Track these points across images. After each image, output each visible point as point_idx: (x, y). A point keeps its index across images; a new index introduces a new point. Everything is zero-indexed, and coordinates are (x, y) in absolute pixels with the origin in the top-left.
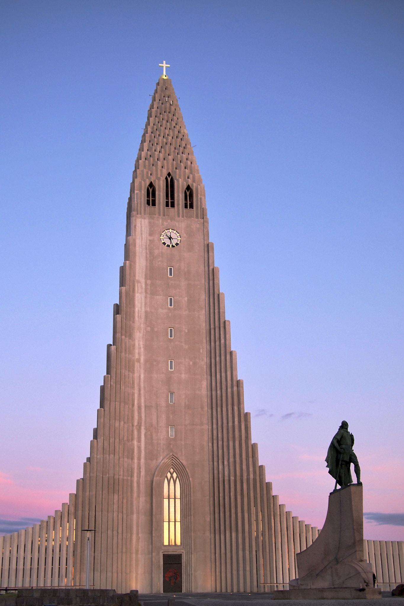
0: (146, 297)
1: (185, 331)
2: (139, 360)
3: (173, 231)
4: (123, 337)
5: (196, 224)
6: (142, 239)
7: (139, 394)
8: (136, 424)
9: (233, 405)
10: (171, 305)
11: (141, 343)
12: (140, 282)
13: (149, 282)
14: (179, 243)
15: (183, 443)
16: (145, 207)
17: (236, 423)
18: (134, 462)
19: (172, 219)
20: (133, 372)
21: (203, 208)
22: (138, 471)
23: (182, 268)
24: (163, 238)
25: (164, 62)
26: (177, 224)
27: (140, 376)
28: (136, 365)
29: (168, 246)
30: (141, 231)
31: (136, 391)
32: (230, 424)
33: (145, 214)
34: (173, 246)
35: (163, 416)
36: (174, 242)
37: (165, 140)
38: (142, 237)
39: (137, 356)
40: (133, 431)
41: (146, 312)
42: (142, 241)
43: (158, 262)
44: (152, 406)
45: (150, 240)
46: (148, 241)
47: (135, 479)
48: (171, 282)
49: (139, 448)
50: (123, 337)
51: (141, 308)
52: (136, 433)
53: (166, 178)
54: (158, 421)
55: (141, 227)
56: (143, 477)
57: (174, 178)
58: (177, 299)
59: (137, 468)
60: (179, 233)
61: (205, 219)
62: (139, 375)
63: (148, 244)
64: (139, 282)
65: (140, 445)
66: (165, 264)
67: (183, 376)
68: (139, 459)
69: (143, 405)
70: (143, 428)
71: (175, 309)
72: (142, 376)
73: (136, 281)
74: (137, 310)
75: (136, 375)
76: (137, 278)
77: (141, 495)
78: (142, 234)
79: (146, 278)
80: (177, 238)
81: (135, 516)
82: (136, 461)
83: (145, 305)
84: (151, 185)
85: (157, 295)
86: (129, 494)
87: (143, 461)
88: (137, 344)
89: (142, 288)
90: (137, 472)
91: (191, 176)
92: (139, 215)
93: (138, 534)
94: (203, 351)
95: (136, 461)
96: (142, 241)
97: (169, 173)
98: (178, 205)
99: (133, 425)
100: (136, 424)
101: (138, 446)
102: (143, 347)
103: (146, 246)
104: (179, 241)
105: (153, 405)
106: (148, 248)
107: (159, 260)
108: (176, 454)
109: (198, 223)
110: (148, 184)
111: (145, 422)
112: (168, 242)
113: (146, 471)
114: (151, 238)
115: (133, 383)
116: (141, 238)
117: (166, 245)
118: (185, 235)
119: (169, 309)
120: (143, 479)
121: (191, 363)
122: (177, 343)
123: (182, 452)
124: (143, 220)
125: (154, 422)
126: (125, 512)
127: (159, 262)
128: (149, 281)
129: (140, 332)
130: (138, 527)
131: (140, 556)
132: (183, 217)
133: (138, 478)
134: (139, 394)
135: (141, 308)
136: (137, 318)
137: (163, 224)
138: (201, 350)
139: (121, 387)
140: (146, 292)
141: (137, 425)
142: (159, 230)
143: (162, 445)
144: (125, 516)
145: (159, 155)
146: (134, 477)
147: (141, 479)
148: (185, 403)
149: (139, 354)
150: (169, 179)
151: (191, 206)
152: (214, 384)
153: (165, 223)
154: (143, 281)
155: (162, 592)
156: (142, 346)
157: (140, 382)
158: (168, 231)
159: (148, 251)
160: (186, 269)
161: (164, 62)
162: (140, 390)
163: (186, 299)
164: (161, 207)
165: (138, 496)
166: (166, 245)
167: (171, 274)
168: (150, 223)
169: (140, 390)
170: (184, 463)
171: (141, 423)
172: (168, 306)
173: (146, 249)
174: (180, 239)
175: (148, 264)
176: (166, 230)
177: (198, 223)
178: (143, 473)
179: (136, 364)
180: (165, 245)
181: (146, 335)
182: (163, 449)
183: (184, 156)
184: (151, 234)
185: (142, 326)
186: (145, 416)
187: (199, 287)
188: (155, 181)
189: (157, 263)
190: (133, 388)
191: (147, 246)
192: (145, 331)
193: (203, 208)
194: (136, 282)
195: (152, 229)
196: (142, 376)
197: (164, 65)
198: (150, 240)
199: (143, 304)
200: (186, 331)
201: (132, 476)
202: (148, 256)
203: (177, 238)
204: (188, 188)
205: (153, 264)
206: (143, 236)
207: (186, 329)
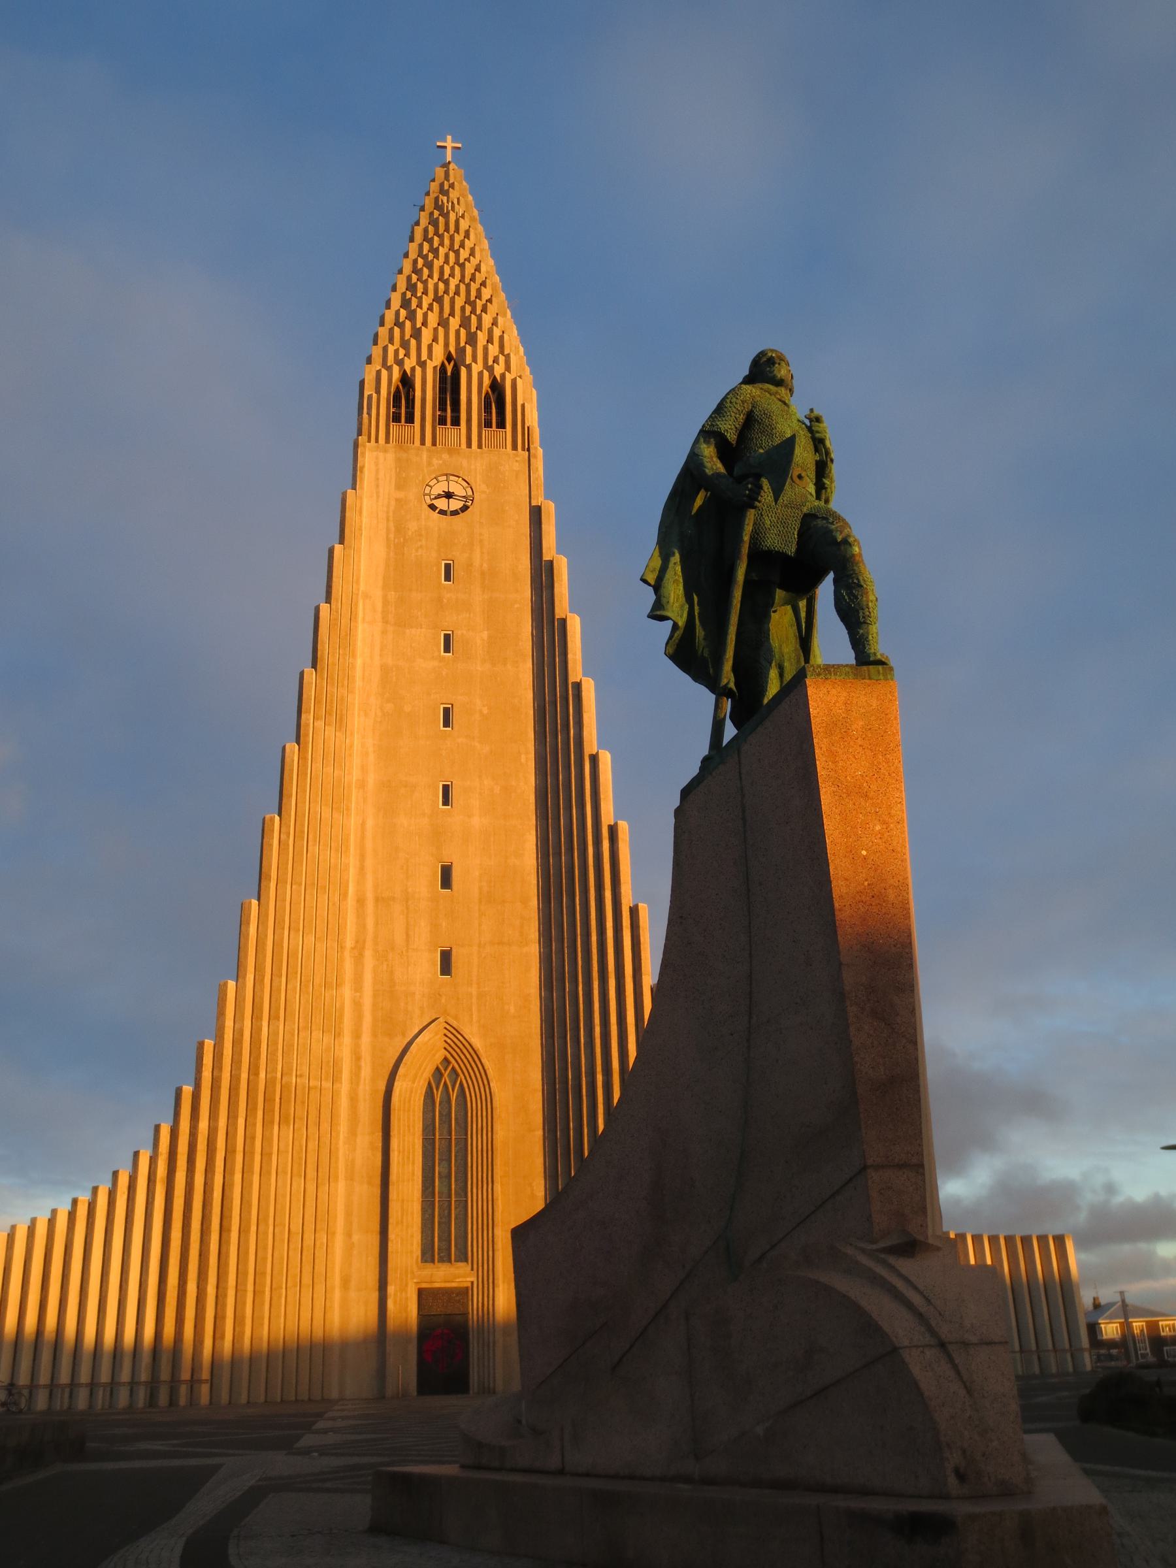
0: (384, 632)
1: (481, 712)
2: (362, 785)
4: (320, 724)
6: (378, 497)
7: (362, 869)
8: (349, 943)
13: (392, 596)
15: (474, 993)
16: (388, 426)
21: (528, 428)
23: (477, 562)
25: (449, 138)
26: (465, 463)
27: (363, 824)
29: (442, 512)
31: (352, 861)
33: (387, 441)
35: (423, 924)
37: (441, 286)
38: (378, 493)
39: (356, 774)
40: (341, 961)
41: (385, 669)
42: (377, 501)
43: (417, 551)
44: (393, 899)
45: (396, 500)
46: (393, 503)
47: (345, 1087)
48: (449, 595)
49: (357, 1005)
50: (320, 724)
52: (348, 966)
54: (407, 935)
56: (367, 1082)
58: (462, 634)
62: (361, 822)
63: (392, 508)
64: (366, 596)
66: (434, 554)
67: (477, 821)
68: (357, 1035)
69: (370, 896)
70: (368, 953)
72: (370, 823)
74: (359, 661)
75: (353, 822)
76: (362, 587)
78: (378, 486)
79: (385, 587)
81: (341, 1187)
82: (347, 1039)
83: (381, 650)
84: (407, 381)
85: (412, 627)
87: (366, 1039)
93: (349, 1235)
94: (527, 758)
95: (347, 1039)
99: (341, 948)
100: (349, 943)
101: (354, 1001)
102: (374, 752)
103: (388, 512)
105: (396, 896)
106: (391, 519)
107: (419, 543)
108: (456, 1018)
109: (517, 461)
112: (442, 504)
114: (400, 495)
116: (375, 495)
117: (437, 511)
118: (483, 487)
119: (442, 659)
120: (367, 1088)
121: (497, 790)
122: (460, 740)
123: (471, 1015)
124: (381, 455)
125: (399, 938)
126: (311, 1173)
127: (420, 550)
128: (393, 593)
129: (366, 715)
130: (348, 1214)
131: (353, 1294)
133: (352, 1083)
137: (429, 464)
138: (523, 756)
140: (385, 621)
141: (352, 948)
142: (421, 478)
144: (311, 1188)
147: (361, 1087)
148: (480, 888)
150: (449, 368)
151: (501, 424)
153: (435, 461)
154: (378, 594)
155: (415, 1393)
156: (371, 749)
157: (363, 838)
159: (391, 524)
160: (485, 565)
161: (449, 138)
162: (362, 857)
163: (485, 635)
165: (353, 1132)
166: (437, 511)
168: (398, 460)
169: (362, 857)
170: (477, 1042)
171: (364, 941)
172: (440, 651)
173: (388, 520)
175: (392, 554)
177: (517, 461)
178: (366, 1071)
181: (381, 722)
184: (399, 487)
186: (377, 924)
187: (516, 606)
189: (414, 551)
191: (391, 514)
192: (379, 714)
193: (528, 428)
195: (404, 475)
196: (370, 823)
197: (449, 143)
198: (396, 500)
200: (485, 711)
201: (336, 1079)
202: (392, 536)
205: (403, 554)
206: (381, 490)
207: (484, 706)
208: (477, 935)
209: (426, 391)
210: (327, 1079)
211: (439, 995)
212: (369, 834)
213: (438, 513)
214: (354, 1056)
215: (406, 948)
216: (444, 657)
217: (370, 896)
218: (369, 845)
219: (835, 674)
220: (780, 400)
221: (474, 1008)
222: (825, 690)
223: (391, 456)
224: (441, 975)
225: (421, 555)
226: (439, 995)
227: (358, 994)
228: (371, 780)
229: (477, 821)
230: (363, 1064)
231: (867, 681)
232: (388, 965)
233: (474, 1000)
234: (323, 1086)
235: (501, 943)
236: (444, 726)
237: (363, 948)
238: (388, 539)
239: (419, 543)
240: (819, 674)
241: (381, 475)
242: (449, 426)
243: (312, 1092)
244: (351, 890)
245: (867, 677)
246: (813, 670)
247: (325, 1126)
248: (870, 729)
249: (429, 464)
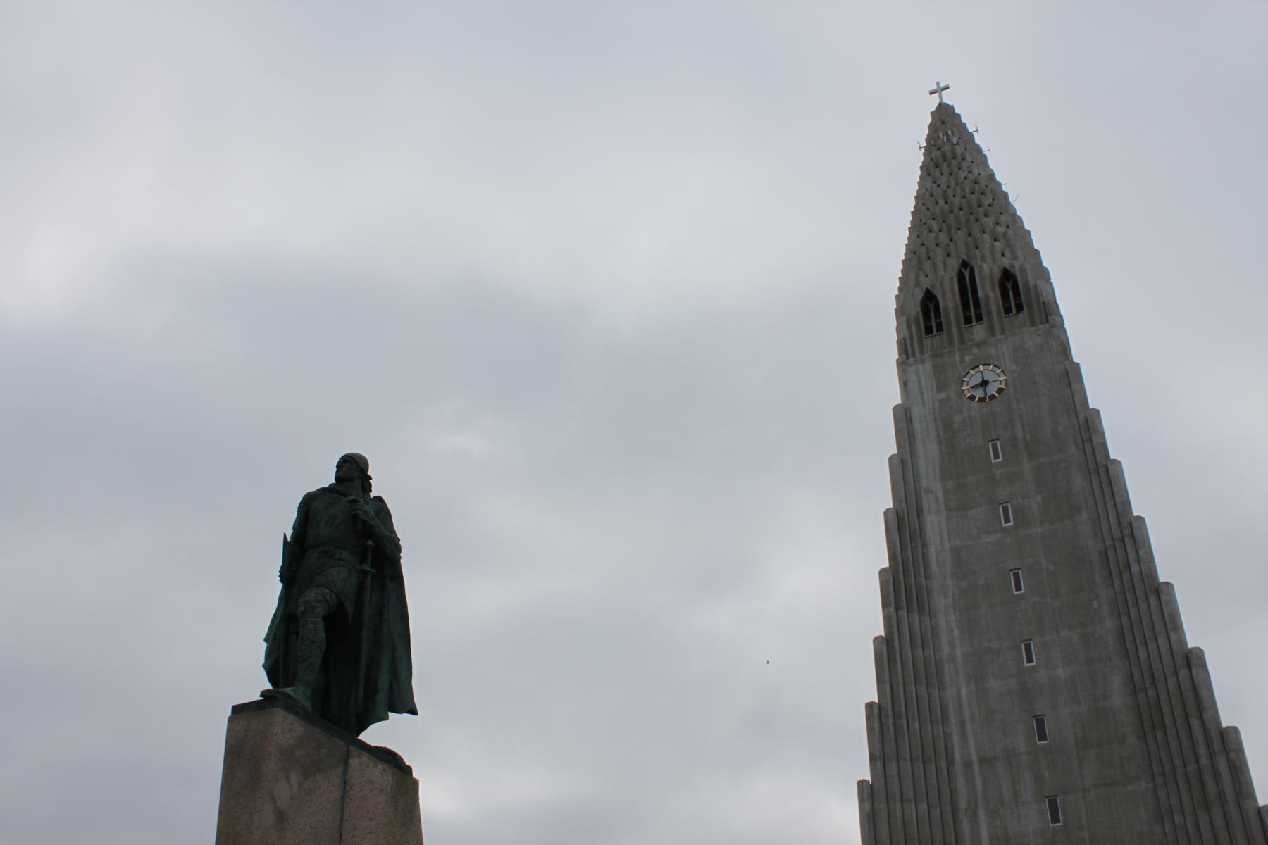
0: (948, 519)
3: (986, 367)
5: (1031, 338)
7: (963, 734)
8: (963, 804)
9: (1187, 716)
10: (1007, 520)
11: (952, 618)
12: (932, 491)
14: (1003, 387)
16: (920, 340)
17: (1204, 761)
19: (979, 345)
20: (941, 686)
24: (968, 387)
27: (959, 693)
28: (947, 668)
29: (981, 400)
30: (920, 388)
31: (954, 729)
32: (1191, 767)
33: (922, 353)
34: (992, 397)
36: (992, 390)
38: (923, 399)
39: (945, 650)
41: (956, 551)
42: (924, 406)
51: (942, 544)
52: (965, 826)
53: (961, 276)
55: (919, 381)
57: (975, 267)
60: (999, 368)
61: (1051, 321)
64: (928, 491)
67: (1061, 672)
69: (974, 758)
70: (981, 812)
71: (1016, 527)
73: (922, 490)
74: (932, 550)
75: (950, 693)
76: (924, 484)
78: (922, 393)
80: (997, 378)
88: (944, 624)
89: (937, 501)
91: (1007, 253)
92: (912, 360)
96: (924, 406)
97: (964, 261)
98: (989, 313)
104: (1004, 382)
107: (966, 433)
110: (919, 295)
114: (943, 395)
115: (944, 709)
117: (976, 400)
119: (1004, 530)
124: (920, 367)
127: (968, 438)
129: (945, 595)
132: (1003, 333)
134: (963, 734)
135: (942, 544)
136: (934, 567)
137: (962, 361)
139: (911, 725)
140: (949, 509)
141: (966, 810)
142: (957, 375)
145: (937, 237)
149: (951, 645)
150: (967, 274)
152: (1136, 675)
153: (967, 358)
154: (937, 486)
156: (954, 625)
158: (976, 370)
159: (939, 423)
162: (962, 724)
164: (954, 329)
167: (996, 457)
168: (935, 367)
169: (962, 724)
171: (976, 800)
173: (935, 420)
174: (1005, 378)
176: (972, 369)
179: (946, 668)
180: (974, 400)
183: (989, 222)
184: (941, 387)
185: (950, 582)
188: (933, 286)
190: (945, 720)
194: (922, 494)
196: (964, 691)
198: (941, 401)
199: (945, 534)
202: (941, 433)
203: (997, 378)
204: (1007, 277)
206: (925, 395)
209: (949, 300)
212: (965, 702)
213: (978, 401)
216: (1005, 528)
217: (974, 758)
218: (967, 713)
223: (928, 366)
225: (970, 443)
228: (958, 652)
229: (1061, 672)
236: (1017, 590)
238: (938, 436)
239: (966, 433)
241: (923, 383)
242: (974, 323)
244: (957, 755)
249: (962, 361)
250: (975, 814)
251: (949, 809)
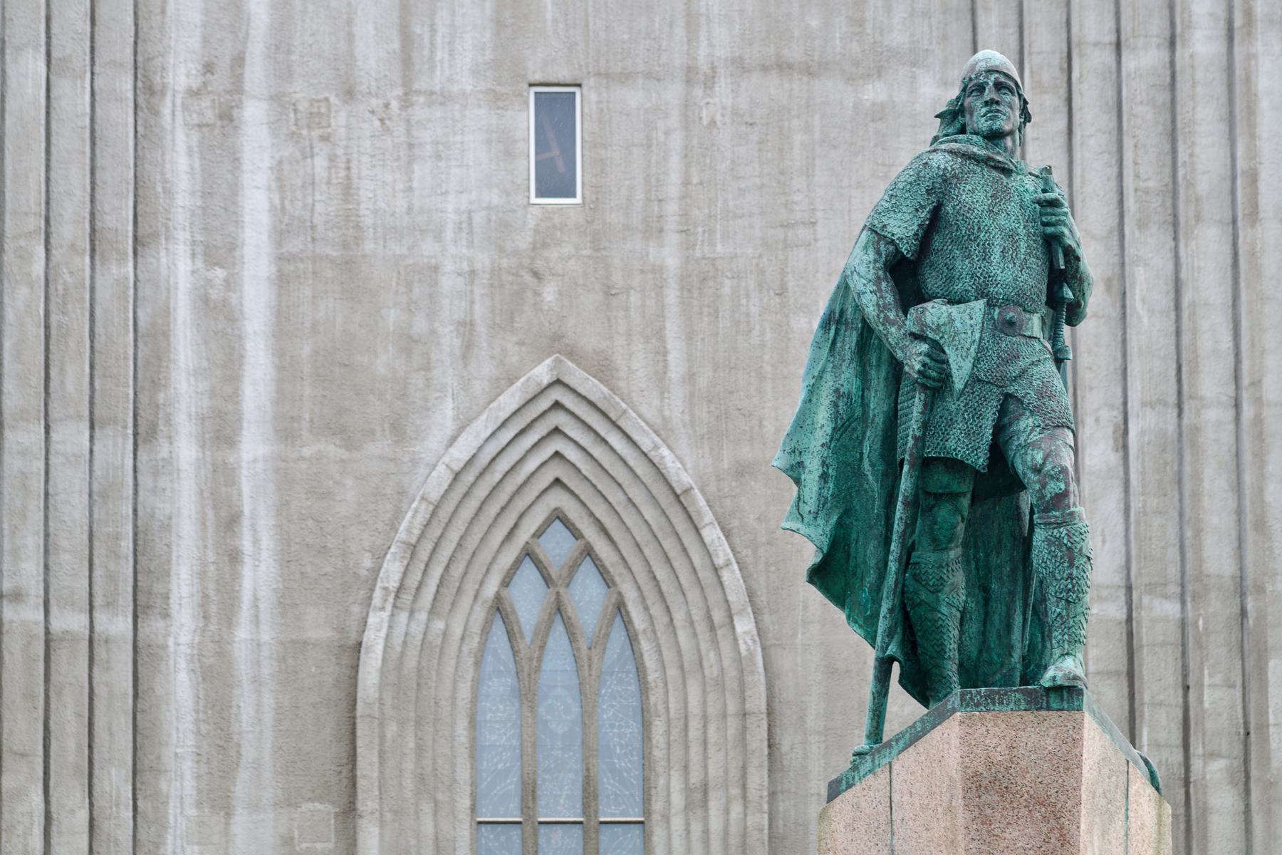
15: (672, 262)
18: (169, 461)
22: (211, 557)
56: (264, 606)
59: (203, 524)
65: (231, 284)
70: (254, 113)
77: (242, 787)
86: (115, 780)
90: (204, 565)
101: (206, 300)
108: (603, 369)
111: (280, 47)
113: (286, 560)
120: (266, 636)
123: (662, 353)
141: (194, 93)
143: (449, 282)
146: (166, 615)
147: (242, 632)
171: (239, 61)
182: (466, 327)
208: (680, 32)
210: (110, 604)
211: (536, 275)
214: (210, 514)
215: (399, 91)
219: (1001, 703)
220: (995, 168)
221: (673, 328)
222: (984, 729)
224: (540, 194)
226: (536, 275)
227: (220, 273)
230: (246, 545)
231: (1043, 713)
232: (332, 159)
233: (672, 296)
234: (98, 628)
235: (783, 67)
237: (237, 87)
240: (977, 705)
243: (61, 657)
245: (1044, 705)
246: (971, 698)
247: (115, 780)
248: (1041, 783)
250: (228, 117)
251: (126, 84)
